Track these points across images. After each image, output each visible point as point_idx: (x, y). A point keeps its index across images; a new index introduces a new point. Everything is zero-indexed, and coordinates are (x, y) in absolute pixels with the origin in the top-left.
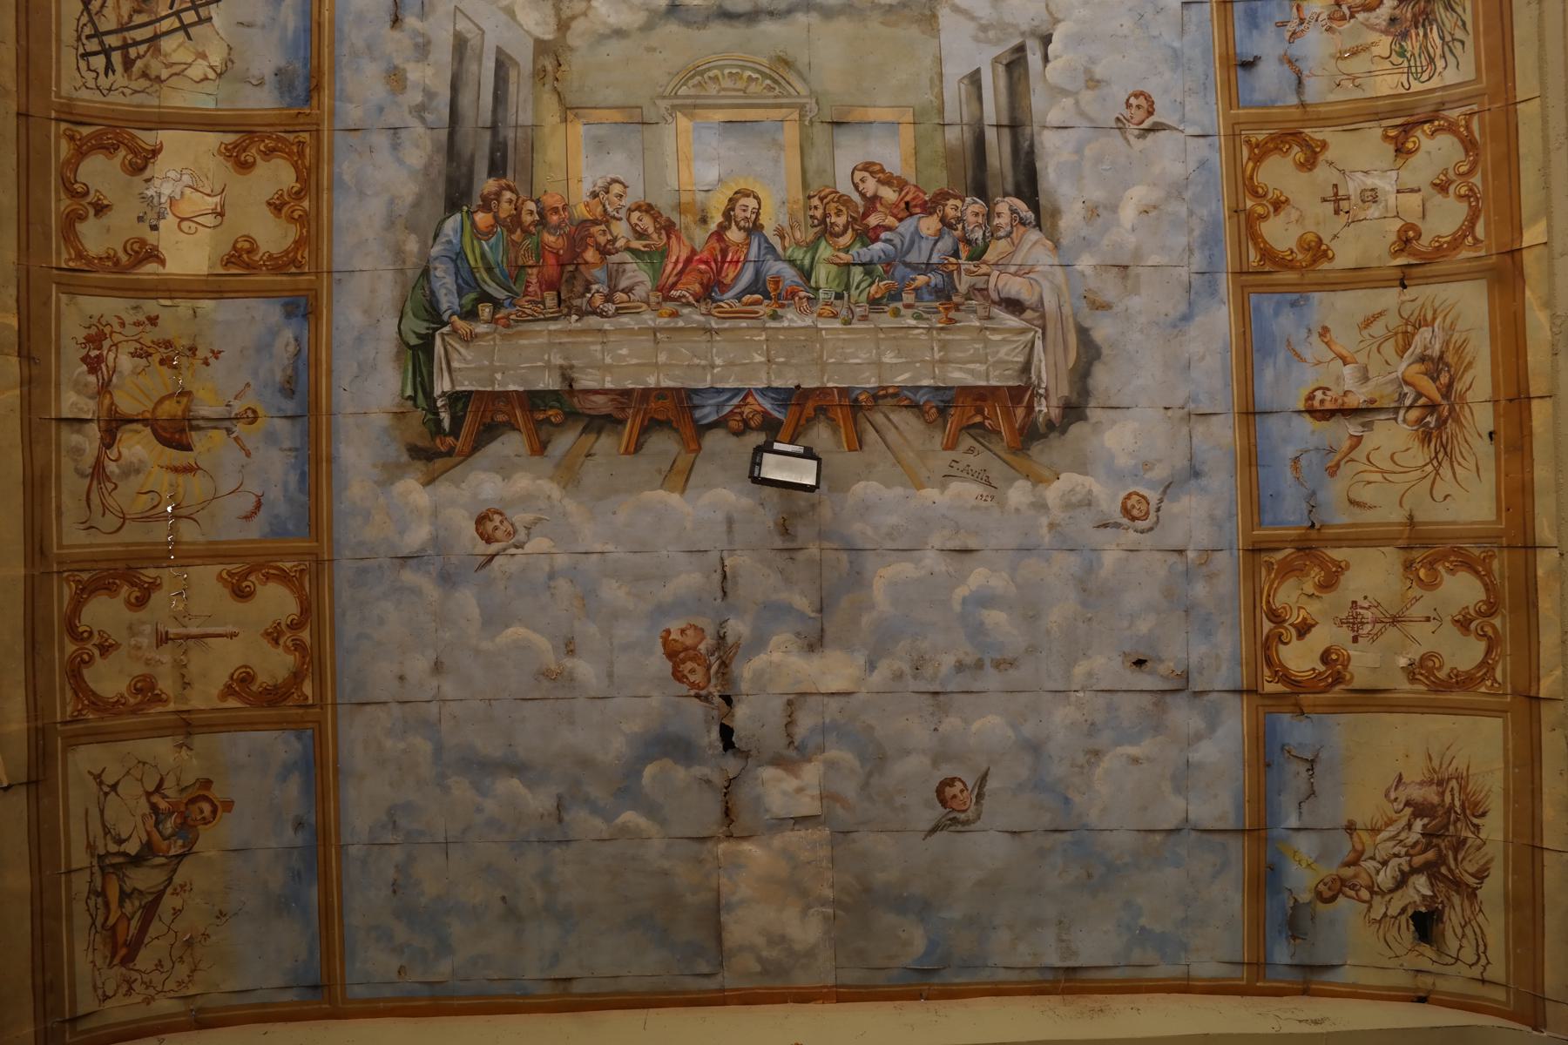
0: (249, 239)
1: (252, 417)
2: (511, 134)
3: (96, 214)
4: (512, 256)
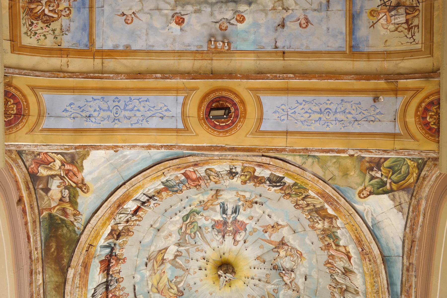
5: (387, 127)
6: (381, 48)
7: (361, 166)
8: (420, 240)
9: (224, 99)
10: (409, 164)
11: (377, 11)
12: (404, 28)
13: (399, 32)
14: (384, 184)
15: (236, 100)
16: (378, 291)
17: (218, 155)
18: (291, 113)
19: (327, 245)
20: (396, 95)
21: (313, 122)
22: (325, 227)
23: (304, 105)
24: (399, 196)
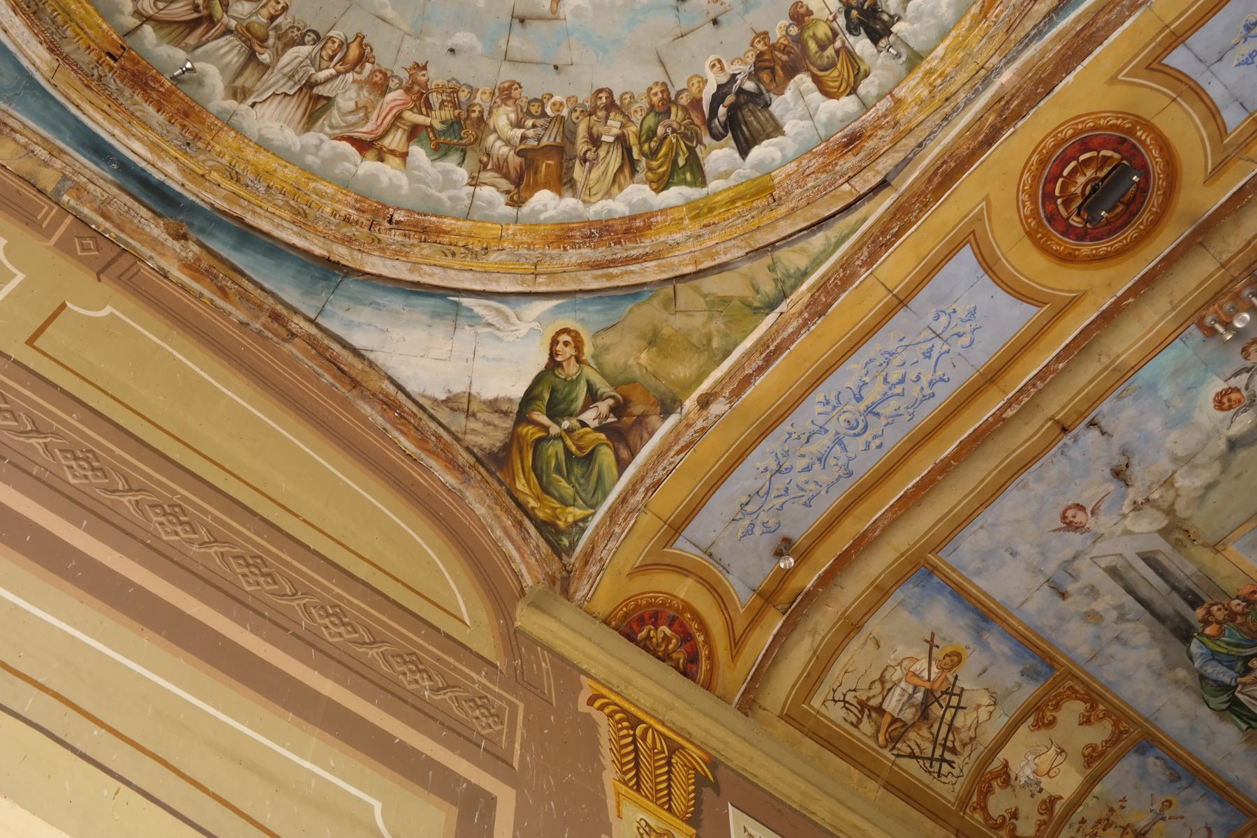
0: (1087, 747)
1: (1169, 803)
2: (1189, 583)
3: (1016, 819)
4: (1245, 630)
5: (706, 527)
6: (874, 626)
7: (646, 392)
8: (345, 404)
9: (1120, 222)
10: (571, 509)
11: (949, 670)
12: (874, 696)
13: (874, 682)
14: (555, 412)
15: (1086, 248)
16: (238, 181)
17: (999, 73)
18: (933, 346)
19: (427, 99)
20: (760, 594)
21: (867, 379)
22: (492, 138)
23: (922, 389)
24: (495, 426)
